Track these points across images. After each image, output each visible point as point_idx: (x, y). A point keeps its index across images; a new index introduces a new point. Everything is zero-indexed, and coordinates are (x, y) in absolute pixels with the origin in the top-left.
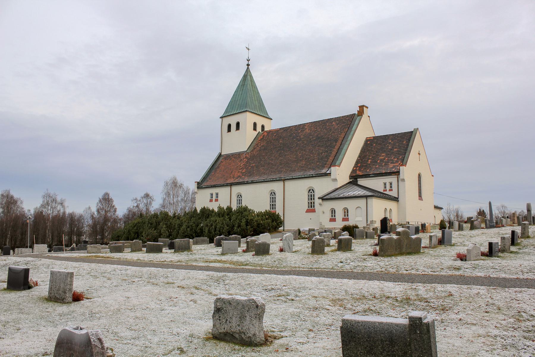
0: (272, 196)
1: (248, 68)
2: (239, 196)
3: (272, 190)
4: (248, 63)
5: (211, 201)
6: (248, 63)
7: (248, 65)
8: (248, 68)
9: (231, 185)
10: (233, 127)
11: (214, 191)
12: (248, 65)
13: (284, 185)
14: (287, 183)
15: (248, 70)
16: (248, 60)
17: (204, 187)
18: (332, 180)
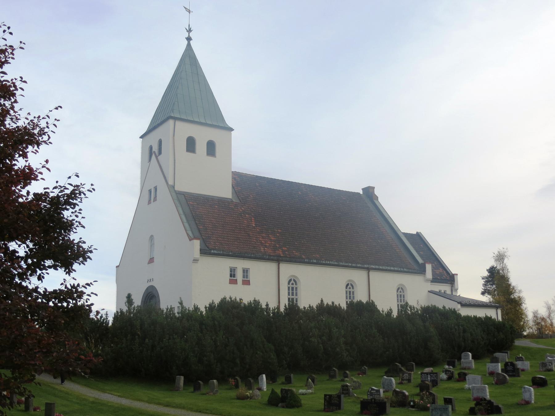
0: (348, 290)
1: (189, 45)
2: (293, 282)
3: (350, 280)
4: (189, 34)
5: (233, 281)
6: (189, 34)
7: (189, 39)
8: (189, 45)
9: (278, 260)
10: (201, 147)
11: (240, 264)
12: (189, 39)
13: (369, 276)
14: (373, 274)
15: (189, 46)
16: (189, 31)
17: (215, 252)
18: (427, 280)
